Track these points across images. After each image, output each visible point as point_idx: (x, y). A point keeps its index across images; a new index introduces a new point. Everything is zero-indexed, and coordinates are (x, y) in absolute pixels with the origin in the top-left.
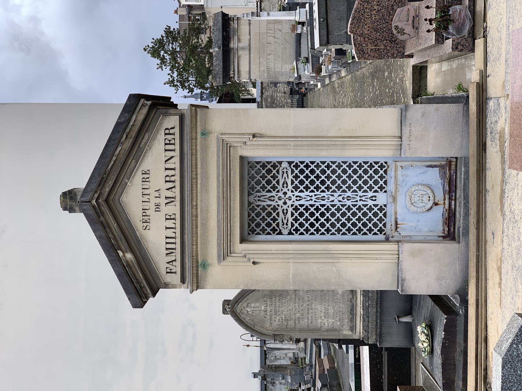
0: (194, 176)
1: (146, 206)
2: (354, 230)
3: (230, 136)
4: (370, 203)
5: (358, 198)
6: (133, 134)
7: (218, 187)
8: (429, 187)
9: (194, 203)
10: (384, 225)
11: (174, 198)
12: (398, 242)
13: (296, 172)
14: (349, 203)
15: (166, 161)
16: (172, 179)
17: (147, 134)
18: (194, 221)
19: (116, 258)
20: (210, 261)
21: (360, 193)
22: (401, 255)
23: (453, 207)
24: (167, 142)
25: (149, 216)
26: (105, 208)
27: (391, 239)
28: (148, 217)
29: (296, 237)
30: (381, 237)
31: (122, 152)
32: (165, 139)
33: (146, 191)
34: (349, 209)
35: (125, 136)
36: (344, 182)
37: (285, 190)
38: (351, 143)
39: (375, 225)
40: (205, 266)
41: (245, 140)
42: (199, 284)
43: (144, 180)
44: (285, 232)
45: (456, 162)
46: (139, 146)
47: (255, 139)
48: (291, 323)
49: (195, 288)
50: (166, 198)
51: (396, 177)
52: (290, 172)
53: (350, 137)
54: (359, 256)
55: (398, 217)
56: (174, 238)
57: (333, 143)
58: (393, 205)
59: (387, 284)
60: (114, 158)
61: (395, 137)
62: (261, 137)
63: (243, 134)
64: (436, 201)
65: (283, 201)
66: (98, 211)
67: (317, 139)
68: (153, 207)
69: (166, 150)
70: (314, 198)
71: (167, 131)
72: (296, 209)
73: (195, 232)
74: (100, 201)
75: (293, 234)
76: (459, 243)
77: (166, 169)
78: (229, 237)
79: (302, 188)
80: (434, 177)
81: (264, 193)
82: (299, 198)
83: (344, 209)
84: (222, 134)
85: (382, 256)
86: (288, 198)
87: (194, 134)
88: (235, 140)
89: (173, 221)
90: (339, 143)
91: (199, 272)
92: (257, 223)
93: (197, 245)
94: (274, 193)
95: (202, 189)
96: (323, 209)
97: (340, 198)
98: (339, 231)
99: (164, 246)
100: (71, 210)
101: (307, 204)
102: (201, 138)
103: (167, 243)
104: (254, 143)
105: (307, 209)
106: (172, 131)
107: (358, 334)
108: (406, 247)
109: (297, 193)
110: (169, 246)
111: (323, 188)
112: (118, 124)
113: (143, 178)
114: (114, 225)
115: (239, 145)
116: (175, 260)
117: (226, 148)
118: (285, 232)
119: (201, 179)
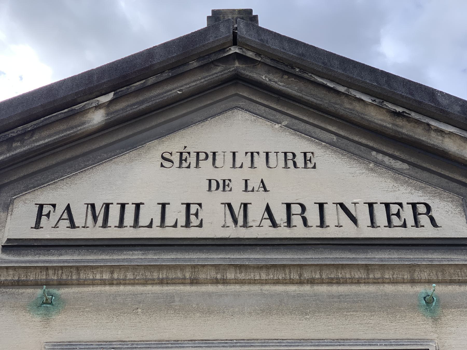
0: (307, 275)
1: (224, 161)
6: (406, 129)
9: (230, 275)
11: (245, 225)
15: (342, 205)
16: (297, 220)
17: (405, 166)
18: (179, 275)
19: (96, 83)
24: (394, 209)
25: (197, 166)
26: (218, 72)
28: (193, 164)
31: (358, 107)
32: (400, 204)
33: (260, 161)
35: (399, 109)
40: (47, 305)
43: (290, 156)
46: (373, 149)
50: (245, 205)
56: (136, 224)
60: (342, 89)
66: (213, 58)
68: (219, 175)
69: (371, 205)
71: (422, 209)
73: (148, 275)
74: (237, 64)
77: (321, 206)
87: (425, 275)
89: (182, 221)
91: (30, 291)
93: (111, 284)
99: (115, 199)
100: (217, 17)
103: (123, 206)
106: (424, 220)
110: (114, 212)
112: (431, 93)
113: (294, 155)
114: (176, 89)
116: (73, 226)
119: (300, 296)
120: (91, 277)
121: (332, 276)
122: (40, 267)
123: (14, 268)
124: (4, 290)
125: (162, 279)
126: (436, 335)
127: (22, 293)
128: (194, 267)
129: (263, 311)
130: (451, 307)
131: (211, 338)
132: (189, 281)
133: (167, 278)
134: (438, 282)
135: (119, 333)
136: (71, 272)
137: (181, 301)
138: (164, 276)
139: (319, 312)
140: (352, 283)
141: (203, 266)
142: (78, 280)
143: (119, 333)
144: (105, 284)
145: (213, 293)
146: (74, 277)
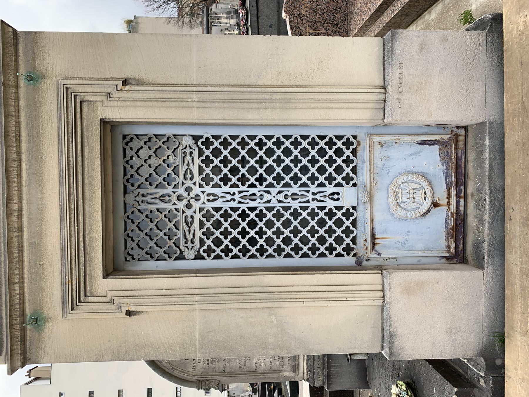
2: (305, 249)
3: (81, 82)
4: (330, 204)
5: (311, 197)
7: (60, 176)
8: (424, 176)
9: (15, 206)
10: (354, 240)
12: (380, 268)
13: (207, 152)
14: (295, 205)
18: (15, 240)
20: (47, 312)
21: (313, 188)
22: (387, 293)
23: (462, 209)
27: (365, 263)
29: (209, 263)
30: (349, 260)
34: (295, 214)
36: (287, 170)
37: (189, 183)
38: (300, 96)
39: (339, 240)
40: (38, 321)
41: (109, 90)
42: (28, 355)
44: (190, 254)
45: (466, 136)
47: (127, 88)
48: (220, 365)
49: (19, 364)
51: (371, 160)
52: (196, 153)
53: (297, 87)
54: (316, 295)
55: (377, 226)
57: (268, 96)
58: (367, 206)
59: (361, 342)
61: (376, 87)
62: (138, 85)
63: (106, 79)
64: (436, 200)
65: (185, 202)
67: (240, 92)
70: (237, 197)
72: (208, 216)
75: (203, 258)
76: (480, 266)
78: (82, 268)
79: (217, 179)
80: (431, 160)
81: (152, 190)
82: (214, 197)
83: (287, 215)
84: (66, 78)
85: (357, 295)
86: (197, 197)
88: (89, 89)
90: (278, 97)
92: (131, 243)
93: (23, 282)
94: (169, 190)
95: (30, 179)
96: (252, 215)
97: (281, 197)
98: (279, 250)
101: (226, 206)
102: (26, 86)
104: (124, 95)
105: (226, 215)
107: (301, 375)
108: (397, 279)
109: (208, 189)
111: (252, 180)
115: (99, 98)
117: (74, 104)
118: (190, 254)
119: (29, 161)
120: (18, 296)
121: (14, 139)
122: (11, 329)
123: (11, 346)
124: (28, 349)
125: (19, 250)
126: (54, 78)
127: (30, 337)
128: (9, 231)
129: (40, 186)
130: (35, 65)
131: (59, 218)
132: (20, 233)
133: (18, 247)
134: (17, 70)
135: (56, 274)
136: (14, 309)
137: (34, 238)
138: (17, 249)
139: (40, 150)
140: (19, 127)
141: (8, 224)
142: (20, 304)
143: (56, 274)
144: (23, 286)
145: (28, 217)
146: (18, 307)
